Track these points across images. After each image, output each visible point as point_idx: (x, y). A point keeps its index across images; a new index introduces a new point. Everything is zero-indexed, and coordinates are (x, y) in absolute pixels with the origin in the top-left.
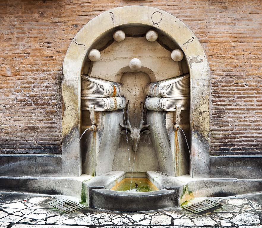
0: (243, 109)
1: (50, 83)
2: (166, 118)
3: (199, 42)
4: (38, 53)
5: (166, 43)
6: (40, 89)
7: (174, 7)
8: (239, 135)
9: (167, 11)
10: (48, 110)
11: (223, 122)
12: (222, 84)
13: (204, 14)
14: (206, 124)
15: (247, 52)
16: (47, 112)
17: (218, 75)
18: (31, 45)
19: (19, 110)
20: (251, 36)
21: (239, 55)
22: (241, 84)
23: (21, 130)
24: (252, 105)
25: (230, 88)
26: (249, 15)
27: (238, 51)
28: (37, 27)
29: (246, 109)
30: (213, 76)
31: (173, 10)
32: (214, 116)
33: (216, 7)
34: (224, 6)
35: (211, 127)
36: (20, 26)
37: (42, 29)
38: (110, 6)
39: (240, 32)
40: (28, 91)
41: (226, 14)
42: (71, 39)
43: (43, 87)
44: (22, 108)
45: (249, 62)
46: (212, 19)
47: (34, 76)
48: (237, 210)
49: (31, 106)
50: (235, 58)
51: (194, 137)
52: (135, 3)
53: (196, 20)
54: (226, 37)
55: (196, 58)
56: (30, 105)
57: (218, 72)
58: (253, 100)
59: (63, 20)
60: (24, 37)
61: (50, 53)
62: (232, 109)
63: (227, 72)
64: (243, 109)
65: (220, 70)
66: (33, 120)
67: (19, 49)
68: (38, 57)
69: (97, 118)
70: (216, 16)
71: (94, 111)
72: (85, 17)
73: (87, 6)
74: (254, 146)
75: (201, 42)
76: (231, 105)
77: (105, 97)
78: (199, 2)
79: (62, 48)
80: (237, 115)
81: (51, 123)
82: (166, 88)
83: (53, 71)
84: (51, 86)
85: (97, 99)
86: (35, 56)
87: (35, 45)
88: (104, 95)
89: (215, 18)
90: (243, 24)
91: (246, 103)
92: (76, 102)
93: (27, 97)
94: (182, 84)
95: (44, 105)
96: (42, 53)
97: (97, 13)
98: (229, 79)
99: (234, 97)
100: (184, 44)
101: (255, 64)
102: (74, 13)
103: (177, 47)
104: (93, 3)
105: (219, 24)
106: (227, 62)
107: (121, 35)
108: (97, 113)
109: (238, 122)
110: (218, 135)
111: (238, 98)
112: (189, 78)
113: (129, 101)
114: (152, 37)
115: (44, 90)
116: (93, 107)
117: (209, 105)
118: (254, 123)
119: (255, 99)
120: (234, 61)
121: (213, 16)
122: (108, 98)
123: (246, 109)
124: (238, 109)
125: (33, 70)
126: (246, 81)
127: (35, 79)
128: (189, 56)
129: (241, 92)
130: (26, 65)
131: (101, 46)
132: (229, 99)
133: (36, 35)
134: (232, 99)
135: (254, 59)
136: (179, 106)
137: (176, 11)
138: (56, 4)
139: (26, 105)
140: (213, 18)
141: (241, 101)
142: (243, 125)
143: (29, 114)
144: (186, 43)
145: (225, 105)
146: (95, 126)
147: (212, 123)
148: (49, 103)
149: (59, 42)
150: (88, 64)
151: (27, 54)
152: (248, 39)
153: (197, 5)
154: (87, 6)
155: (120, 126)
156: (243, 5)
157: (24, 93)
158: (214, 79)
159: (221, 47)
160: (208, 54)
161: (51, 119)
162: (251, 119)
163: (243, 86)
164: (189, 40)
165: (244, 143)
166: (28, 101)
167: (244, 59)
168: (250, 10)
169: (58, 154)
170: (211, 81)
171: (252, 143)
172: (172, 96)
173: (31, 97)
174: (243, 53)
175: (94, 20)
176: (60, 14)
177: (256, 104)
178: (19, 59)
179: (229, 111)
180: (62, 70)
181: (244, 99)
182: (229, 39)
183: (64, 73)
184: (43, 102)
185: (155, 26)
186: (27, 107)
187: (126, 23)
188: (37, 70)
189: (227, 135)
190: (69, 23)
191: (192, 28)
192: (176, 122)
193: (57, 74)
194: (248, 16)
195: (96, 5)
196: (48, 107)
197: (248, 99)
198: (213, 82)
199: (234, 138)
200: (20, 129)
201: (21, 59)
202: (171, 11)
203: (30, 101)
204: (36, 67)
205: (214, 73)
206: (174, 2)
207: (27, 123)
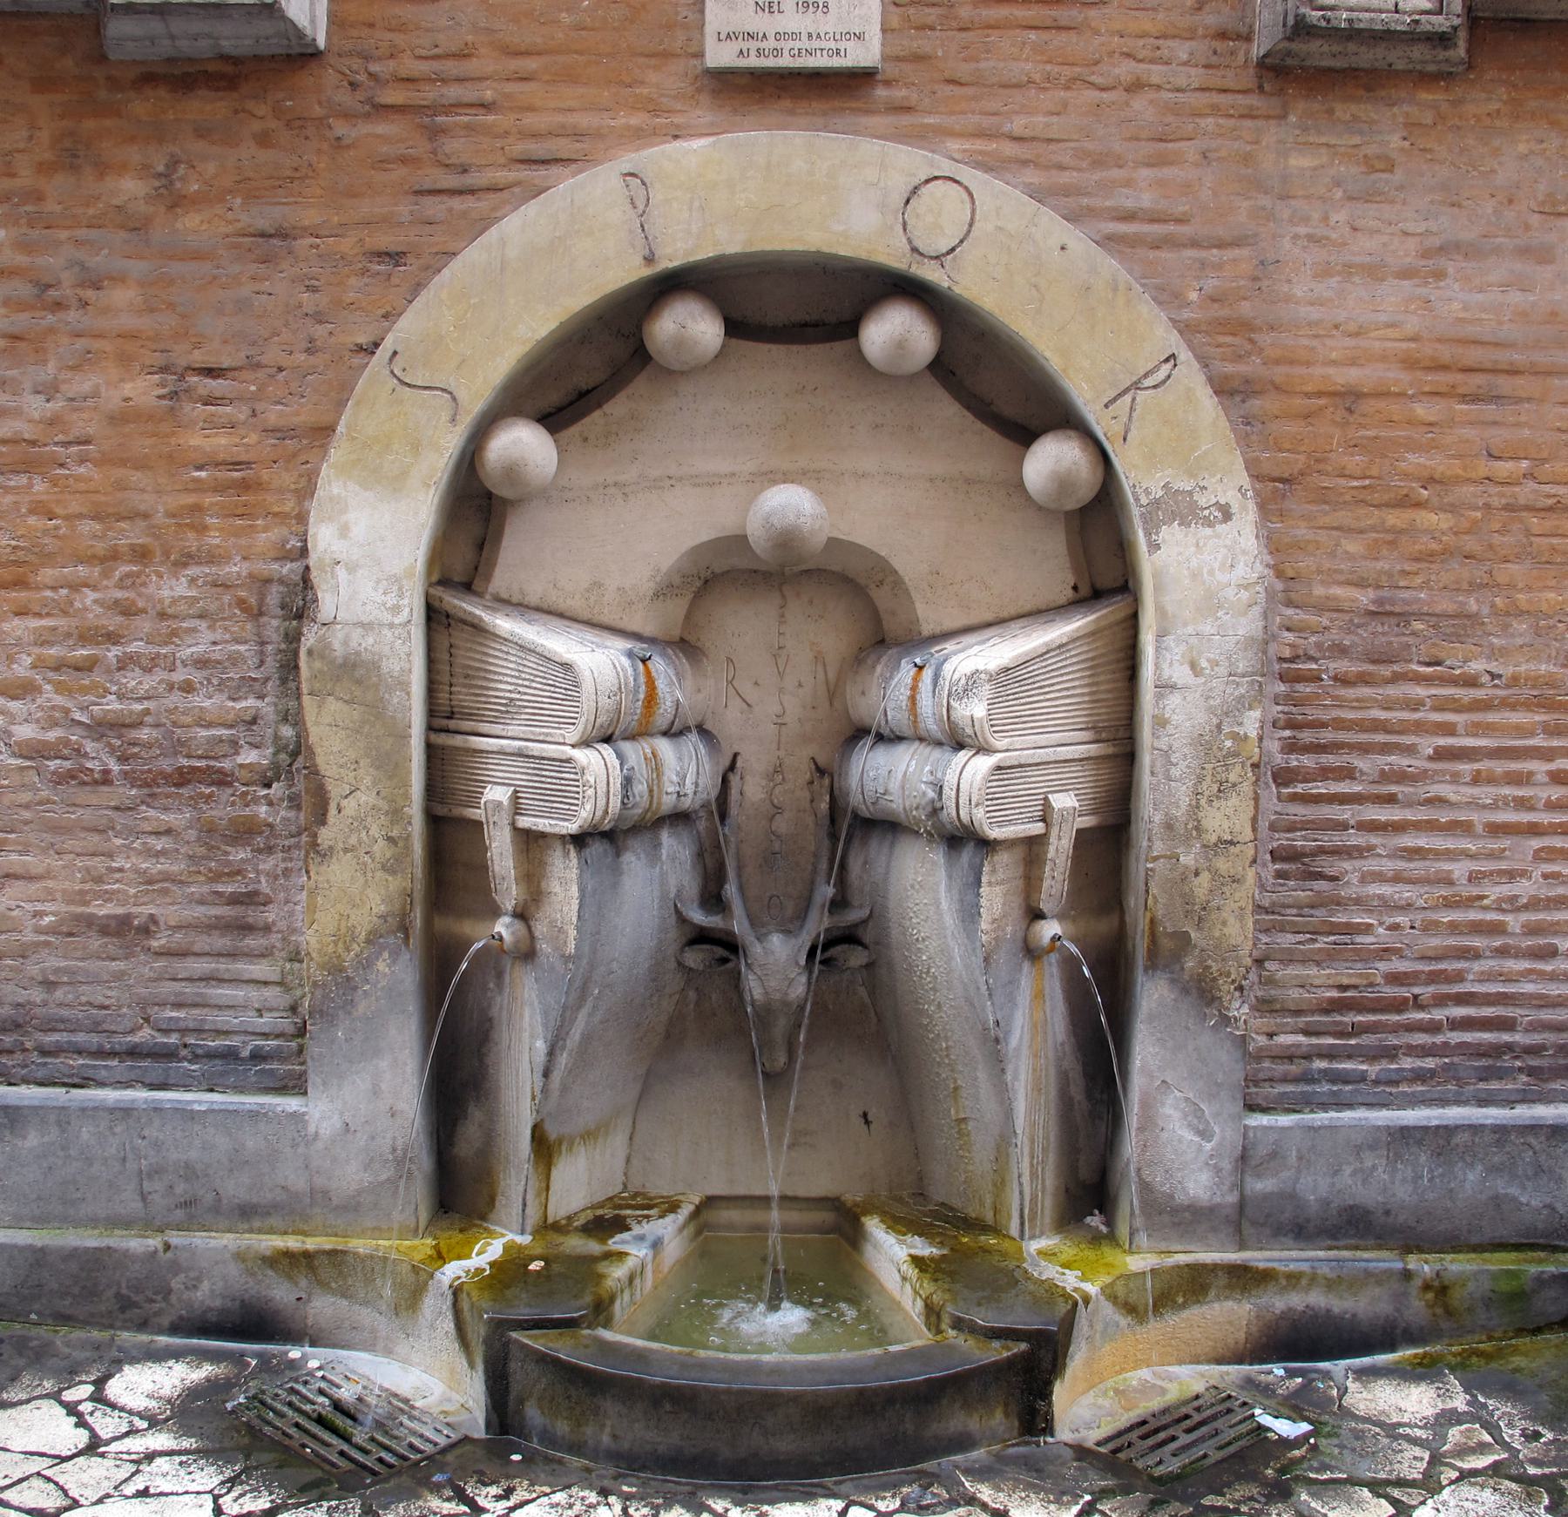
0: (1465, 828)
1: (227, 636)
2: (984, 879)
3: (1210, 391)
4: (148, 442)
5: (995, 386)
6: (160, 674)
7: (1052, 147)
8: (1431, 989)
9: (1009, 176)
10: (213, 813)
13: (1245, 204)
14: (1231, 920)
15: (1510, 465)
16: (210, 829)
17: (1321, 608)
18: (97, 386)
19: (27, 815)
20: (1541, 358)
21: (1458, 481)
22: (1457, 672)
23: (43, 938)
24: (1522, 804)
25: (1393, 691)
26: (1535, 220)
27: (1453, 457)
28: (137, 268)
29: (1479, 829)
30: (1290, 612)
31: (1047, 168)
32: (1286, 866)
33: (1325, 159)
34: (1378, 157)
35: (1265, 939)
36: (21, 259)
37: (172, 282)
38: (628, 127)
39: (1471, 331)
40: (84, 690)
42: (360, 349)
43: (178, 662)
44: (48, 801)
45: (1516, 526)
46: (1296, 237)
47: (119, 594)
48: (1411, 1462)
49: (105, 789)
50: (1435, 500)
51: (1152, 996)
52: (792, 112)
53: (1194, 244)
54: (1384, 358)
55: (1190, 493)
56: (96, 782)
57: (1319, 591)
58: (1531, 774)
60: (51, 330)
61: (223, 441)
62: (1399, 827)
63: (1380, 593)
64: (1465, 828)
66: (117, 875)
67: (17, 413)
68: (141, 465)
70: (1326, 219)
71: (516, 830)
72: (457, 203)
74: (1516, 1058)
75: (1224, 389)
76: (1391, 799)
78: (1221, 121)
79: (302, 413)
80: (1428, 863)
81: (234, 900)
82: (986, 690)
83: (245, 558)
84: (235, 660)
85: (536, 748)
86: (123, 463)
87: (128, 389)
90: (1491, 278)
91: (1486, 793)
92: (389, 765)
93: (79, 731)
94: (1092, 659)
95: (189, 782)
96: (173, 441)
97: (540, 173)
99: (1410, 750)
100: (1115, 400)
101: (1555, 541)
103: (1065, 419)
105: (1339, 273)
108: (530, 843)
111: (1441, 754)
112: (1132, 621)
113: (736, 755)
114: (901, 345)
115: (188, 688)
116: (506, 803)
117: (1256, 799)
118: (1524, 917)
119: (1539, 767)
120: (1428, 518)
121: (1306, 220)
123: (1479, 829)
124: (1431, 826)
125: (114, 556)
126: (1494, 654)
127: (128, 610)
128: (1140, 481)
130: (67, 518)
131: (554, 398)
133: (128, 322)
135: (1550, 509)
136: (1064, 801)
137: (1065, 178)
138: (262, 110)
139: (73, 777)
140: (1302, 230)
141: (1455, 778)
142: (1454, 928)
143: (96, 838)
146: (519, 926)
148: (220, 771)
149: (280, 369)
151: (70, 443)
152: (1520, 381)
155: (682, 920)
156: (1496, 152)
157: (59, 700)
160: (1267, 468)
161: (239, 872)
162: (1505, 890)
163: (1471, 682)
164: (1146, 376)
165: (1456, 1037)
166: (86, 755)
167: (1487, 506)
168: (1542, 188)
169: (281, 1090)
170: (1273, 649)
171: (1506, 1037)
172: (1018, 742)
173: (102, 728)
174: (1483, 467)
177: (1545, 795)
178: (23, 480)
179: (1374, 840)
180: (304, 552)
181: (1476, 766)
182: (1396, 377)
183: (314, 574)
185: (930, 273)
186: (83, 795)
187: (731, 249)
188: (142, 555)
189: (1355, 987)
190: (347, 245)
191: (1168, 297)
193: (268, 581)
194: (1527, 227)
195: (530, 121)
196: (211, 795)
197: (1500, 767)
198: (1287, 653)
199: (1399, 1006)
200: (39, 931)
201: (37, 480)
202: (1032, 176)
203: (99, 757)
204: (131, 535)
206: (1055, 119)
207: (82, 898)
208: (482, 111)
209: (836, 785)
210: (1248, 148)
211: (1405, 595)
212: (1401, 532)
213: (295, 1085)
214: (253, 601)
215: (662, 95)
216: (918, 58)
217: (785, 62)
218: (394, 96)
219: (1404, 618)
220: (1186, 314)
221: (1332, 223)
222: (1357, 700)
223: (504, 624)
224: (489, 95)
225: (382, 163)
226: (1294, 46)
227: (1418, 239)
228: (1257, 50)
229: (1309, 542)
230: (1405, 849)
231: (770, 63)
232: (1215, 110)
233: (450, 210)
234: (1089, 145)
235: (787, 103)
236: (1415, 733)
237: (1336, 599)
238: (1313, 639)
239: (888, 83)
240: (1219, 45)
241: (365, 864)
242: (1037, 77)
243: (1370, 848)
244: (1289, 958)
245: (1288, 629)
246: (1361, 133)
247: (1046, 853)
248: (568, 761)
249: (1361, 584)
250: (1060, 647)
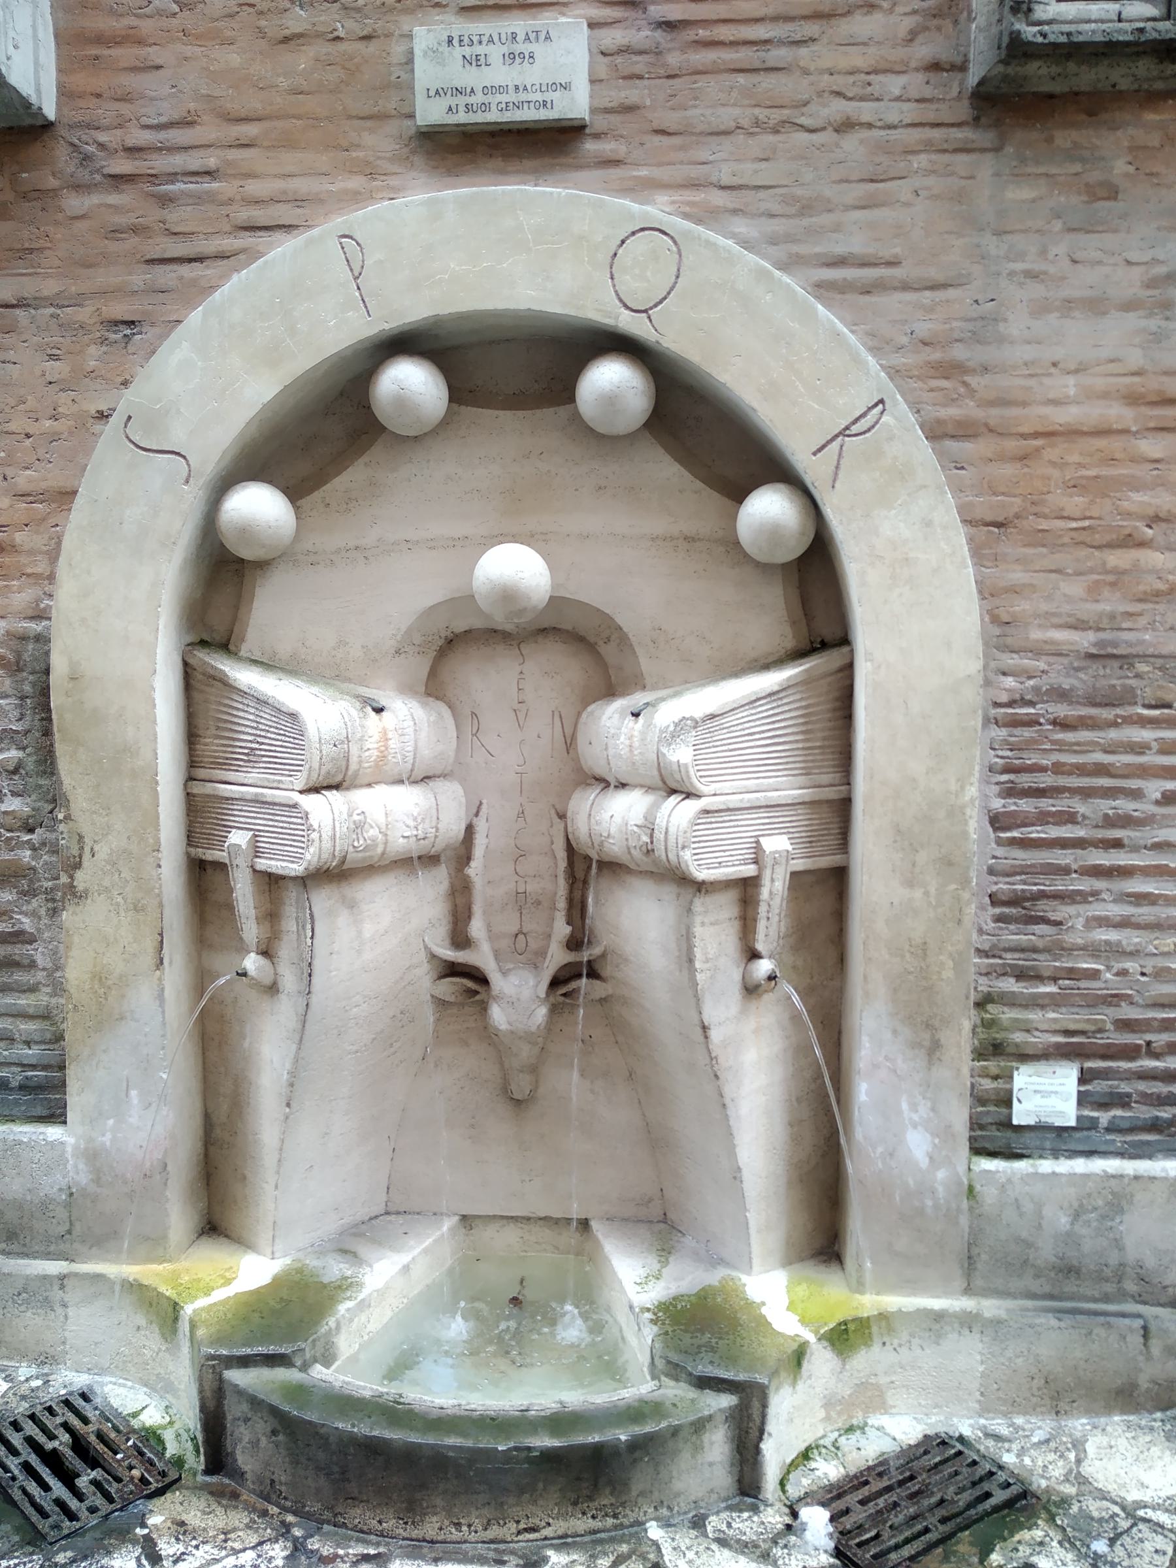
5: (707, 437)
7: (762, 194)
11: (1057, 949)
12: (1062, 710)
17: (1036, 651)
25: (1113, 734)
32: (1006, 910)
35: (983, 980)
41: (1109, 240)
46: (1012, 274)
50: (1161, 540)
52: (503, 172)
53: (906, 287)
54: (1105, 395)
57: (1036, 635)
59: (46, 293)
62: (1125, 872)
65: (1055, 620)
69: (271, 916)
70: (1043, 252)
71: (255, 871)
72: (185, 270)
73: (199, 199)
75: (936, 433)
76: (1117, 844)
77: (315, 790)
78: (934, 157)
88: (305, 774)
89: (1037, 267)
94: (806, 707)
97: (262, 238)
98: (1111, 678)
99: (1136, 794)
102: (113, 247)
103: (774, 469)
104: (234, 176)
106: (1104, 564)
107: (411, 382)
108: (271, 882)
109: (1164, 954)
110: (1028, 1031)
114: (610, 400)
120: (1154, 558)
121: (1021, 256)
122: (332, 795)
129: (1152, 759)
132: (1106, 806)
134: (1125, 805)
136: (777, 844)
140: (1019, 266)
144: (837, 436)
145: (1080, 843)
146: (262, 961)
147: (987, 957)
149: (28, 436)
150: (223, 580)
153: (917, 182)
154: (199, 199)
158: (1010, 679)
159: (1062, 465)
160: (981, 513)
175: (236, 289)
176: (31, 251)
179: (1100, 884)
182: (1118, 413)
192: (760, 947)
193: (23, 638)
195: (254, 188)
198: (1004, 698)
199: (1131, 1052)
202: (741, 226)
205: (1009, 640)
206: (764, 165)
208: (207, 178)
209: (570, 830)
210: (963, 182)
211: (1126, 636)
212: (1124, 572)
213: (56, 1115)
215: (379, 158)
216: (628, 109)
217: (493, 116)
218: (122, 166)
219: (1126, 660)
220: (899, 360)
221: (1051, 256)
222: (1078, 744)
223: (245, 676)
224: (212, 162)
225: (115, 233)
226: (1010, 70)
227: (1141, 269)
228: (973, 78)
229: (1024, 585)
230: (1129, 895)
231: (480, 118)
232: (929, 147)
233: (181, 278)
234: (799, 192)
235: (498, 162)
236: (1139, 777)
237: (1052, 642)
238: (1032, 682)
239: (597, 136)
240: (933, 77)
241: (118, 904)
242: (745, 123)
243: (1095, 893)
244: (1010, 1000)
245: (1004, 674)
246: (1083, 160)
247: (758, 894)
248: (295, 806)
249: (1079, 625)
250: (770, 695)
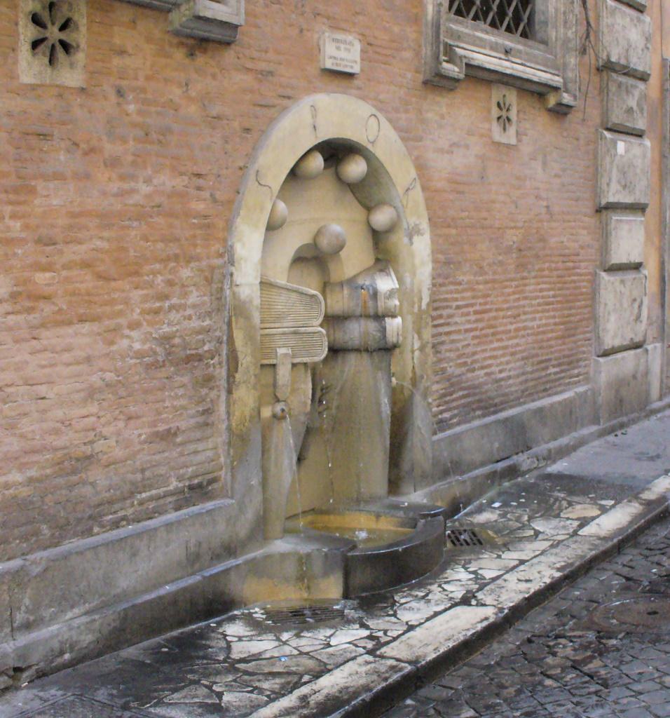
115: (190, 318)
125: (168, 259)
127: (170, 283)
139: (153, 365)
184: (188, 352)
188: (176, 257)
204: (174, 249)
214: (209, 276)
